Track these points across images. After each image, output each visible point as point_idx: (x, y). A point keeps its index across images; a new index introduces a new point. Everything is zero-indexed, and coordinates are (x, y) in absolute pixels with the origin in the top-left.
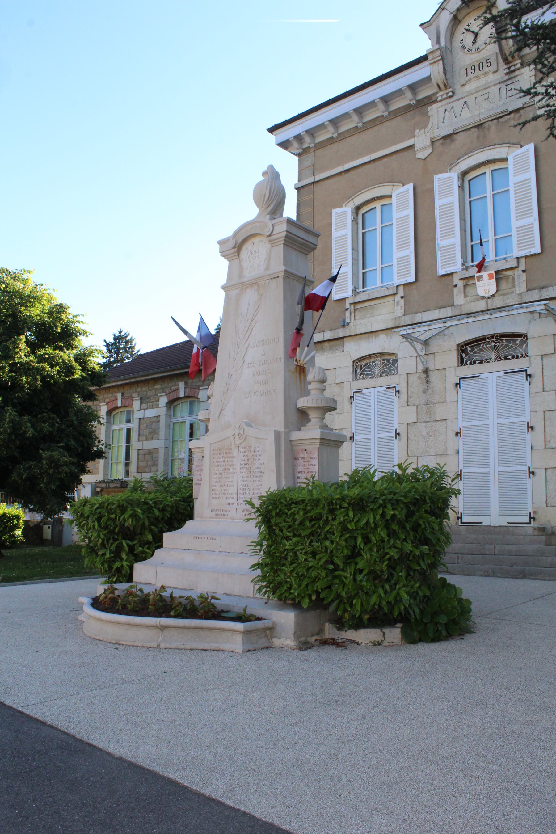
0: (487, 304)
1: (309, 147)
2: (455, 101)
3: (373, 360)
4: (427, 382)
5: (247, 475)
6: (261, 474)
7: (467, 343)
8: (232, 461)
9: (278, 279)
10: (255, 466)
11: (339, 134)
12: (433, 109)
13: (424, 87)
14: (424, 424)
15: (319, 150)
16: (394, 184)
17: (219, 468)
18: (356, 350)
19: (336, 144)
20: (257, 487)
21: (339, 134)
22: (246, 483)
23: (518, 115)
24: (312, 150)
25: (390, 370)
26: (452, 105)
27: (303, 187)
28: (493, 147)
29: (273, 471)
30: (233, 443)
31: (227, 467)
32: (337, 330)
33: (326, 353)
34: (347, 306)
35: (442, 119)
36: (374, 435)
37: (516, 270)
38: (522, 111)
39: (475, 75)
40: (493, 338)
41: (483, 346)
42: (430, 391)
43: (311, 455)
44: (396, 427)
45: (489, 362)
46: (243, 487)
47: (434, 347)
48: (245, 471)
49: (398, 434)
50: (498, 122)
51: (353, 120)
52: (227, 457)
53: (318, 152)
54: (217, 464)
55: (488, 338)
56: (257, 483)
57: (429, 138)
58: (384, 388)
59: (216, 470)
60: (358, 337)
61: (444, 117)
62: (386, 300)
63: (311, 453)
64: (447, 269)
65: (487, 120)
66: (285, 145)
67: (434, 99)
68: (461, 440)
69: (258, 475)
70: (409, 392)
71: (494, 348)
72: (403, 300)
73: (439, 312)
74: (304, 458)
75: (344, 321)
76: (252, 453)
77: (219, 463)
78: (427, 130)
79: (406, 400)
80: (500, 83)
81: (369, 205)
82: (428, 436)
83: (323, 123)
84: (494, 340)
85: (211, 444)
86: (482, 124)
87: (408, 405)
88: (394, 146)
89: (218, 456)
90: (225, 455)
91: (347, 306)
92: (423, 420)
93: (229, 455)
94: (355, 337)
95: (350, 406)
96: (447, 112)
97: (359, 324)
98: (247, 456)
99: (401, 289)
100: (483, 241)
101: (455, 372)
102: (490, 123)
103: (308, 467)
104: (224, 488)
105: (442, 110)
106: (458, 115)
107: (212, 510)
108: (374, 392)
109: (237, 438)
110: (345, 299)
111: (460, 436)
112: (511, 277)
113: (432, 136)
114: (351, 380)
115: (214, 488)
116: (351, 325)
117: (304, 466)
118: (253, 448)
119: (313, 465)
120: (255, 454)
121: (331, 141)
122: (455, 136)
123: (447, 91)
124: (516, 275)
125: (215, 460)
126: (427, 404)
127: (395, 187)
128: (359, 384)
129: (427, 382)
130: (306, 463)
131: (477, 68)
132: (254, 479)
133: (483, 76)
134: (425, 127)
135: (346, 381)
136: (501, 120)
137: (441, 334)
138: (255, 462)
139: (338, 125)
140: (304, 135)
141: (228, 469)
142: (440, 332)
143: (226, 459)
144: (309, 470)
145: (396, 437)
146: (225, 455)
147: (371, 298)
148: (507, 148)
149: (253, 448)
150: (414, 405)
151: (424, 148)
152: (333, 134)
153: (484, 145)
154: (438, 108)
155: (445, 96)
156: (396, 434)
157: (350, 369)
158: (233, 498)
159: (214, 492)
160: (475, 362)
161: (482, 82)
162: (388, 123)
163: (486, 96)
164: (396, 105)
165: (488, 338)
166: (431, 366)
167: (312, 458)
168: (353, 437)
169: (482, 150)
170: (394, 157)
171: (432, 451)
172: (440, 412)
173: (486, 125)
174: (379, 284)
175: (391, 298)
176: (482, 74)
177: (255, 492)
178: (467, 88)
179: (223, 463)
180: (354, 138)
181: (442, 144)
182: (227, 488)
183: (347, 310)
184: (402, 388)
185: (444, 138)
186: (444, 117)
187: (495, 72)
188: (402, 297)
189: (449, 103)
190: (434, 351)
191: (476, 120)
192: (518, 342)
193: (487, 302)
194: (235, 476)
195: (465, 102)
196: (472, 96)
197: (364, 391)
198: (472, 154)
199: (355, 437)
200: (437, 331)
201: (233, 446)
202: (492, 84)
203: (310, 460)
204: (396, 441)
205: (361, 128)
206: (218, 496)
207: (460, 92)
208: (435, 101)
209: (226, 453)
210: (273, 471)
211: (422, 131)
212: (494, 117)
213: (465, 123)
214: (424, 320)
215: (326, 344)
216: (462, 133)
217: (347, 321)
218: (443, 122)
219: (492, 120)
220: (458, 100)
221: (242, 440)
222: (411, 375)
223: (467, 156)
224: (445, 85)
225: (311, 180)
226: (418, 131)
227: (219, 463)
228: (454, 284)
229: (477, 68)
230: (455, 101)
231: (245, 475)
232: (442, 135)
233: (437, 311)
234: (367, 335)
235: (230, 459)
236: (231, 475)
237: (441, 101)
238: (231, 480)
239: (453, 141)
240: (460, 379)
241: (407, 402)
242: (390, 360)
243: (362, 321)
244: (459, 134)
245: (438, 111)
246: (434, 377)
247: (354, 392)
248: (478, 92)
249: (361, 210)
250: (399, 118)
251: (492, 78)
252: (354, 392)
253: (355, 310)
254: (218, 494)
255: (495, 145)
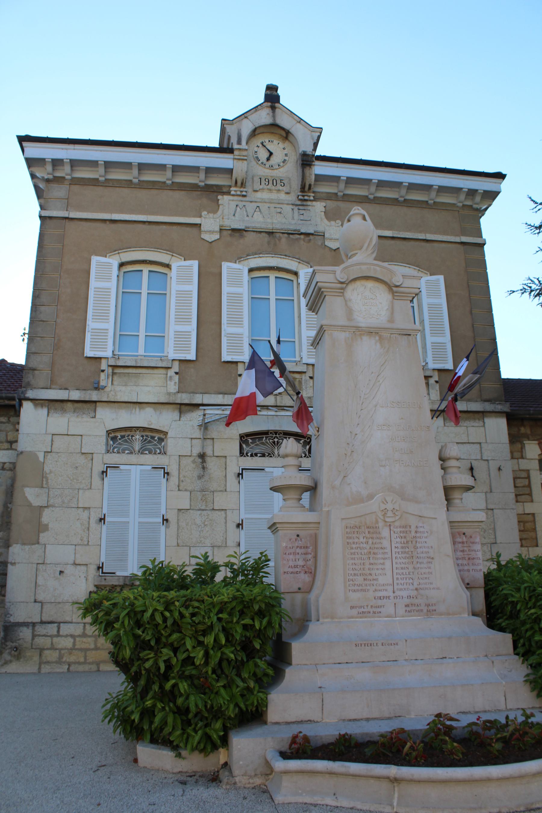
0: (276, 400)
1: (63, 178)
2: (248, 201)
3: (132, 433)
4: (204, 468)
5: (406, 560)
6: (430, 560)
7: (248, 435)
8: (381, 543)
9: (410, 337)
10: (419, 550)
11: (106, 179)
12: (224, 199)
13: (216, 175)
14: (199, 512)
15: (77, 186)
16: (174, 254)
17: (359, 551)
18: (113, 420)
19: (101, 188)
20: (425, 576)
21: (106, 179)
22: (407, 571)
23: (307, 238)
24: (67, 182)
25: (155, 449)
26: (244, 203)
27: (50, 218)
28: (285, 257)
29: (448, 556)
30: (380, 520)
31: (372, 551)
32: (89, 392)
33: (68, 415)
34: (104, 366)
35: (230, 212)
36: (134, 519)
37: (303, 375)
38: (311, 237)
39: (268, 187)
40: (276, 434)
41: (266, 439)
42: (206, 478)
43: (472, 540)
44: (163, 512)
45: (271, 457)
46: (402, 576)
47: (214, 432)
48: (404, 555)
49: (165, 520)
50: (289, 237)
51: (132, 173)
52: (372, 538)
53: (75, 188)
54: (354, 546)
55: (271, 433)
56: (424, 571)
57: (218, 224)
58: (149, 468)
59: (354, 554)
60: (116, 404)
61: (235, 211)
62: (156, 371)
63: (471, 537)
64: (234, 357)
65: (278, 231)
66: (30, 162)
67: (225, 190)
68: (242, 532)
69: (425, 561)
70: (181, 476)
71: (277, 444)
72: (177, 376)
73: (224, 398)
74: (463, 543)
75: (98, 383)
76: (413, 534)
77: (357, 545)
78: (215, 216)
79: (177, 484)
80: (293, 205)
81: (133, 266)
82: (203, 525)
83: (97, 162)
84: (278, 436)
85: (343, 519)
86: (273, 233)
87: (179, 490)
88: (177, 218)
89: (355, 535)
90: (368, 536)
91: (104, 366)
92: (198, 508)
93: (375, 536)
94: (112, 404)
95: (101, 482)
96: (238, 208)
97: (122, 391)
98: (405, 537)
99: (176, 364)
100: (281, 339)
101: (235, 463)
102: (281, 235)
103: (469, 553)
104: (370, 577)
105: (233, 205)
106: (250, 216)
107: (352, 607)
108: (135, 472)
109: (390, 514)
110: (100, 358)
111: (242, 528)
112: (298, 380)
113: (221, 223)
114: (104, 452)
115: (351, 577)
116: (107, 389)
117: (463, 551)
118: (413, 529)
119: (475, 551)
120: (418, 535)
121: (94, 182)
122: (244, 232)
123: (242, 189)
124: (303, 379)
125: (351, 541)
126: (202, 491)
127: (173, 258)
128: (113, 458)
129: (204, 468)
130: (465, 549)
131: (271, 182)
132: (418, 565)
133: (275, 192)
134: (215, 211)
135: (96, 452)
136: (291, 236)
137: (221, 420)
138: (418, 545)
139: (74, 168)
140: (67, 162)
141: (374, 553)
142: (221, 418)
143: (370, 541)
144: (470, 556)
145: (163, 524)
146: (368, 536)
147: (139, 365)
148: (297, 263)
149: (413, 529)
150: (186, 490)
151: (211, 232)
152: (100, 176)
153: (275, 252)
154: (230, 200)
155: (239, 193)
156: (164, 520)
157: (104, 439)
158: (386, 590)
159: (351, 582)
160: (256, 455)
161: (274, 196)
162: (170, 193)
163: (279, 210)
164: (182, 179)
165: (271, 433)
166: (209, 452)
167: (473, 543)
168: (104, 519)
169: (274, 255)
170: (175, 227)
171: (208, 542)
172: (220, 501)
173: (278, 235)
174: (141, 351)
175: (163, 371)
176: (276, 190)
177: (421, 581)
178: (259, 195)
179: (365, 545)
180: (126, 191)
181: (231, 235)
182: (375, 577)
183: (103, 371)
184: (173, 469)
185: (234, 230)
186: (235, 211)
187: (288, 193)
188: (177, 373)
189: (242, 201)
190: (213, 437)
191: (270, 227)
192: (301, 442)
193: (276, 398)
194: (388, 563)
195: (244, 206)
196: (265, 204)
197: (122, 467)
198: (263, 255)
199: (107, 519)
200: (217, 417)
201: (381, 524)
202: (286, 202)
203: (471, 545)
204: (163, 528)
205: (135, 184)
206: (361, 588)
207: (252, 196)
208: (228, 193)
209: (369, 532)
210: (448, 556)
211: (211, 215)
212: (286, 232)
213: (258, 225)
214: (205, 402)
215: (69, 405)
216: (252, 233)
217: (102, 383)
218: (234, 215)
219: (283, 233)
220: (251, 202)
221: (397, 518)
222: (184, 458)
223: (257, 256)
224: (242, 184)
225: (65, 214)
226: (205, 213)
227: (357, 545)
228: (239, 373)
229: (271, 182)
230: (248, 201)
231: (404, 561)
232: (232, 227)
233: (221, 396)
234: (129, 404)
235: (378, 541)
236: (382, 561)
237: (233, 195)
238: (380, 566)
239: (242, 236)
240: (243, 469)
241: (179, 486)
242: (155, 437)
243: (123, 388)
244: (249, 233)
245: (229, 204)
246: (211, 463)
247: (107, 467)
248: (271, 203)
249: (124, 267)
250: (183, 192)
251: (283, 196)
252: (107, 467)
253: (113, 374)
254: (358, 585)
255: (286, 256)
